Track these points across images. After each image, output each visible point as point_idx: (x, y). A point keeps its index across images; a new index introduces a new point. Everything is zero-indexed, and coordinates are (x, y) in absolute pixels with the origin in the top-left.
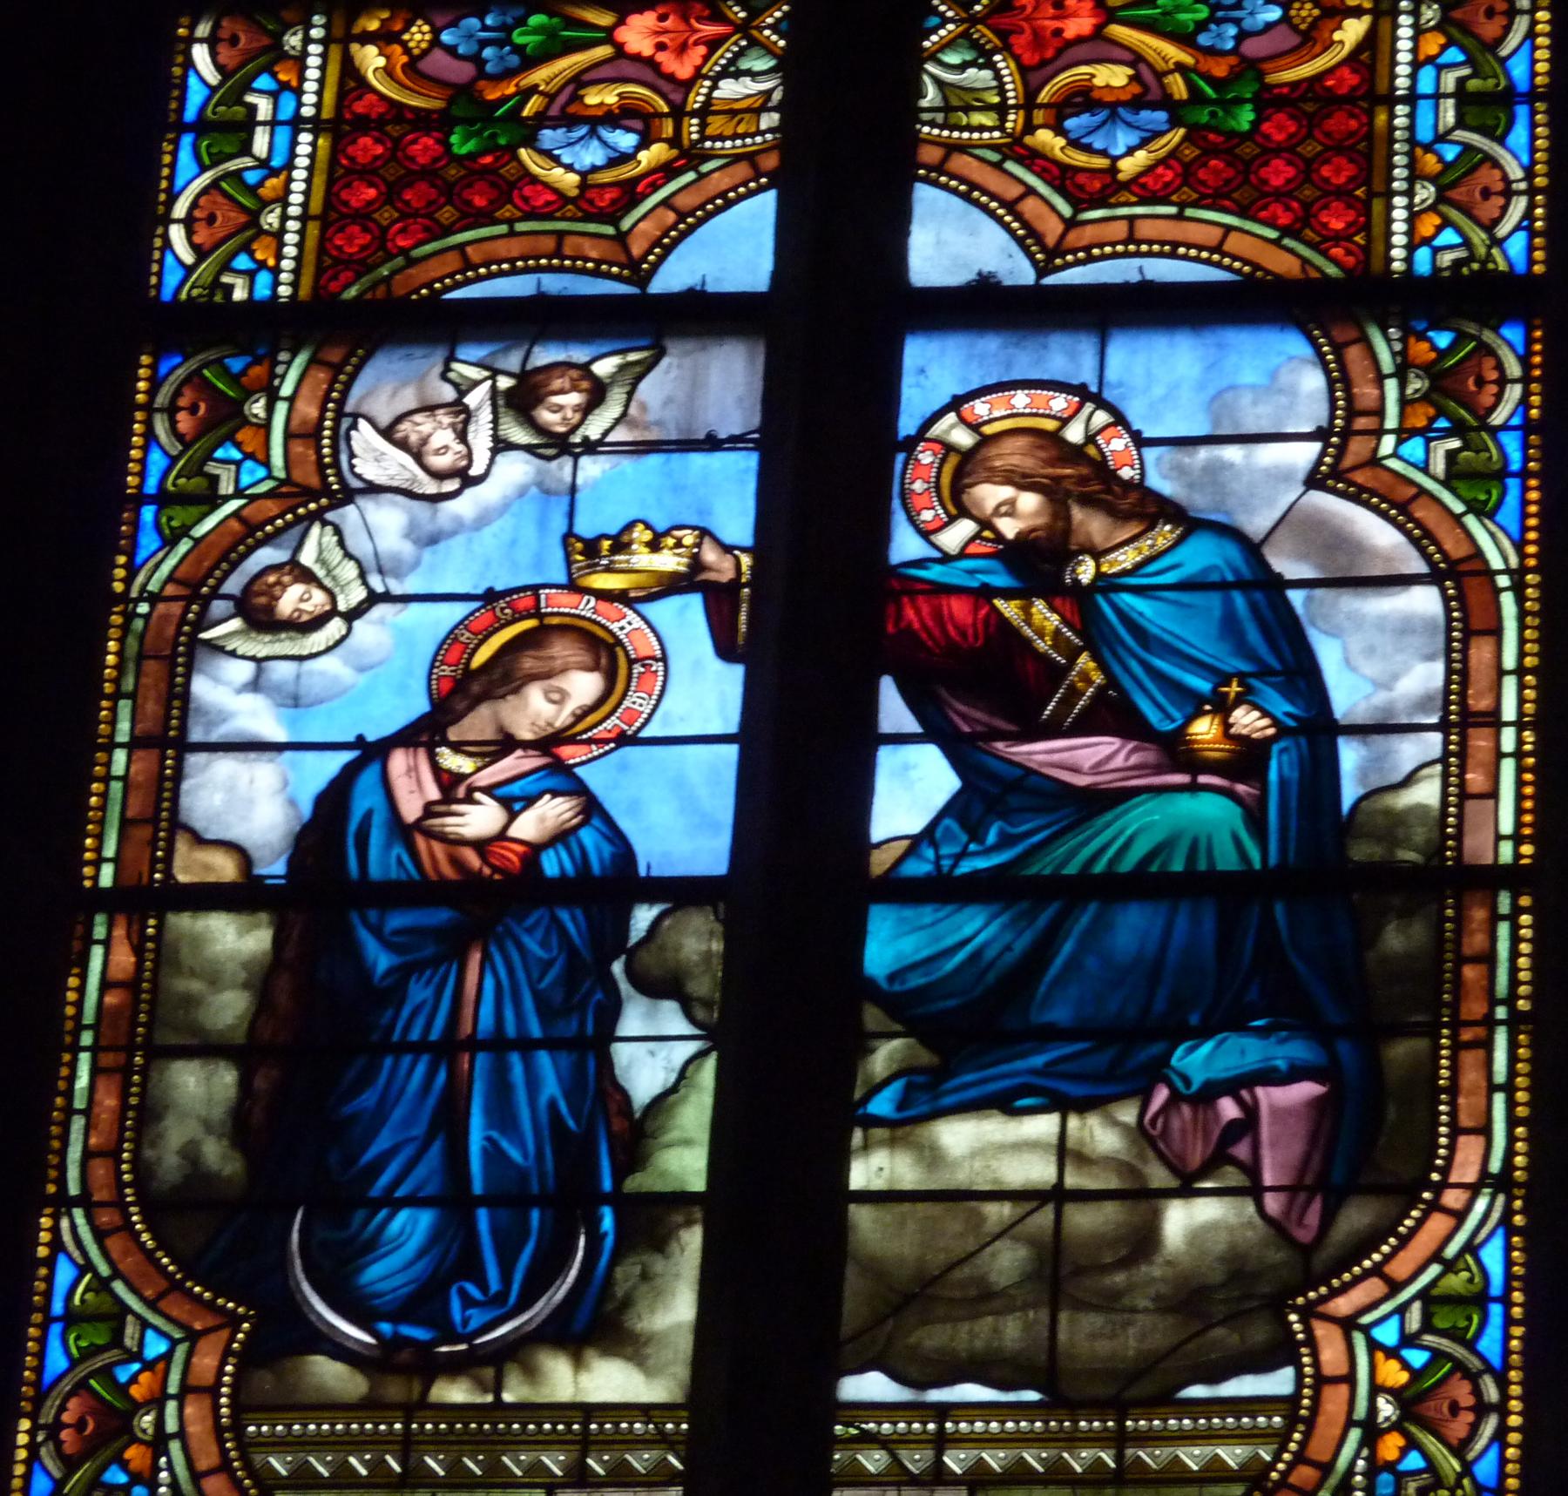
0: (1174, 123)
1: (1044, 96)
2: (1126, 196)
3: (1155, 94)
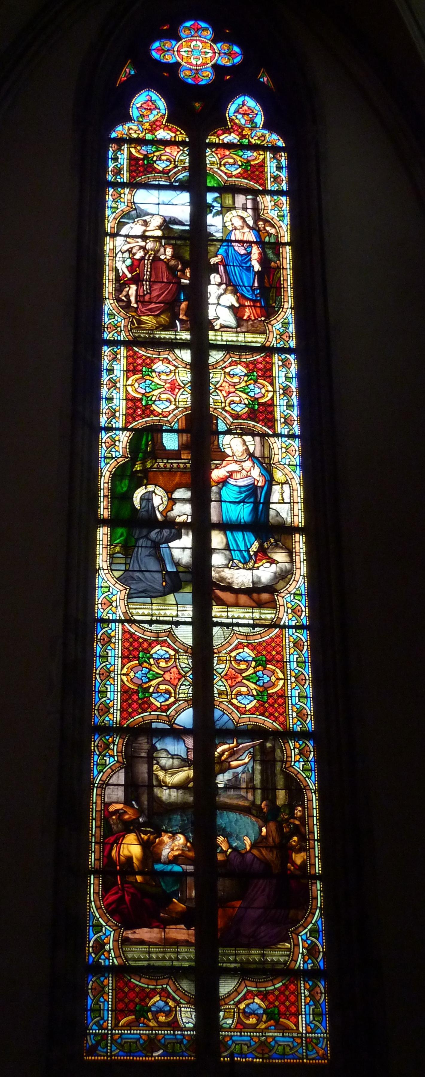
0: (255, 699)
1: (234, 693)
2: (248, 713)
3: (251, 694)
